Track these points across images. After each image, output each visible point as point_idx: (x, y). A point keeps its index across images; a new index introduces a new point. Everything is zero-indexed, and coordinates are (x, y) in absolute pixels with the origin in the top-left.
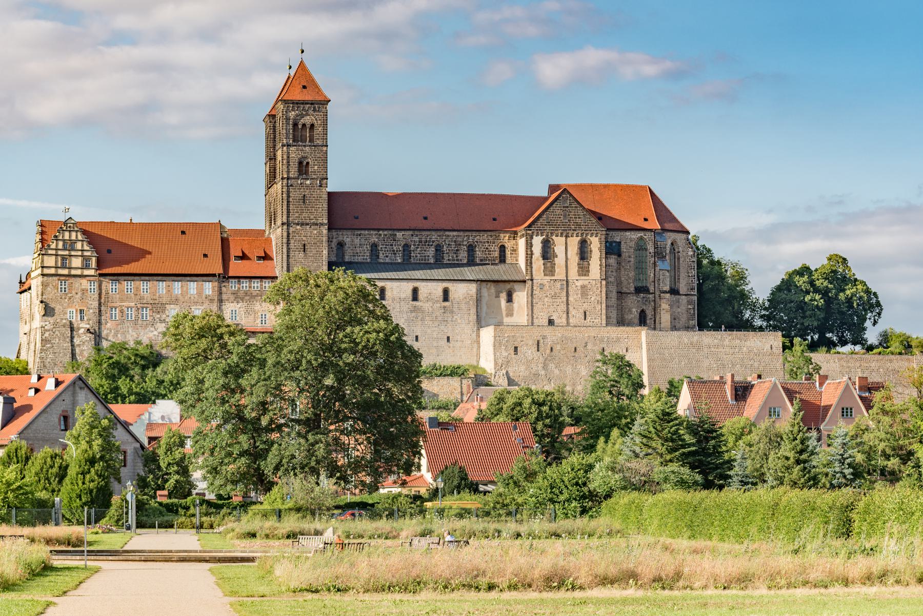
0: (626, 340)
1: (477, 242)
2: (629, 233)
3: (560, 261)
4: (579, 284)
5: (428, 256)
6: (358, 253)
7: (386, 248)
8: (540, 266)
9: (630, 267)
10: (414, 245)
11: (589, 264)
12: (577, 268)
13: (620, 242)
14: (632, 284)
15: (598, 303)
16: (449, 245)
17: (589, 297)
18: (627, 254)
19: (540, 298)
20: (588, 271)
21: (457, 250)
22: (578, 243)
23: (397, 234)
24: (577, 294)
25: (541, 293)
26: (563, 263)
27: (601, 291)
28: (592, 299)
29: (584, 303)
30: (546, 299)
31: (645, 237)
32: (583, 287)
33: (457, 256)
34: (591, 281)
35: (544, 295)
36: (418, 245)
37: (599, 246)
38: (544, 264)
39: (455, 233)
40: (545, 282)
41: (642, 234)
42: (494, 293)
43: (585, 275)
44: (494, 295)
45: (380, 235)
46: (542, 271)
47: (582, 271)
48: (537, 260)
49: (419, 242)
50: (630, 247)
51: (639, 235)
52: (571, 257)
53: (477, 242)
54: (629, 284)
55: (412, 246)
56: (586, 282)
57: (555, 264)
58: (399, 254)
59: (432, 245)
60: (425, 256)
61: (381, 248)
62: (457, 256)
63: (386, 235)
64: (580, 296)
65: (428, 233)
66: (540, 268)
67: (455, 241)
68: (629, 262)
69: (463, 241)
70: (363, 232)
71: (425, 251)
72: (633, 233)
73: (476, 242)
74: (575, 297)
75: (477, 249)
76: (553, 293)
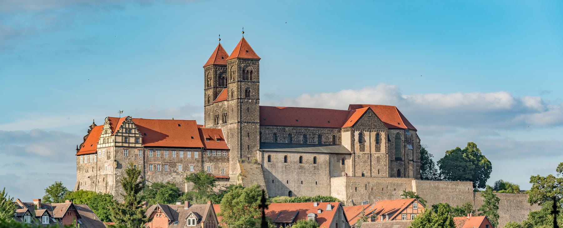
0: (405, 185)
4: (376, 156)
6: (267, 138)
7: (281, 135)
10: (294, 134)
12: (375, 148)
16: (310, 134)
17: (381, 162)
19: (358, 163)
20: (380, 149)
23: (286, 128)
24: (375, 161)
26: (369, 145)
30: (361, 163)
32: (378, 157)
33: (313, 141)
34: (382, 155)
36: (296, 134)
39: (313, 129)
41: (399, 131)
42: (336, 160)
45: (278, 129)
46: (359, 149)
51: (397, 131)
60: (299, 140)
62: (313, 141)
63: (280, 129)
65: (300, 128)
69: (316, 133)
70: (270, 127)
71: (299, 137)
72: (394, 130)
74: (374, 162)
75: (323, 137)
76: (364, 160)
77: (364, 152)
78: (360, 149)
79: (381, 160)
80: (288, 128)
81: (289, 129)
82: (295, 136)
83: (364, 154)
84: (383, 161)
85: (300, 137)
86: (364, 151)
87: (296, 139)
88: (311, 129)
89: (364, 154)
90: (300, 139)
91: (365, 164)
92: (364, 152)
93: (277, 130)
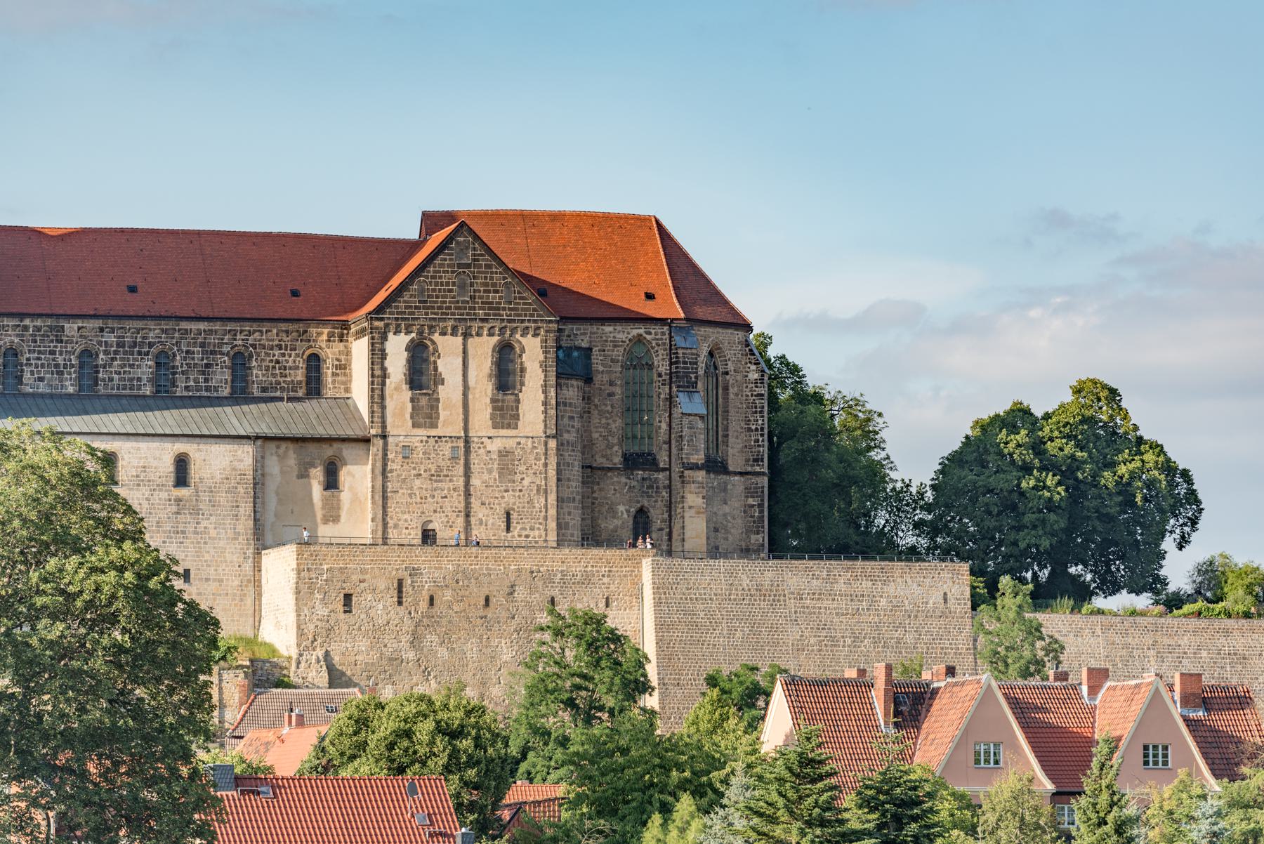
0: (606, 580)
1: (254, 346)
2: (611, 329)
3: (449, 392)
4: (494, 446)
5: (139, 379)
7: (39, 359)
8: (404, 403)
9: (612, 406)
10: (106, 353)
11: (518, 401)
12: (489, 410)
13: (590, 349)
14: (616, 448)
15: (538, 490)
16: (187, 352)
17: (518, 477)
18: (606, 378)
19: (404, 481)
20: (517, 417)
21: (207, 366)
22: (494, 351)
23: (66, 326)
24: (490, 471)
25: (406, 467)
27: (546, 465)
28: (526, 483)
29: (507, 491)
30: (417, 482)
31: (648, 337)
32: (504, 454)
33: (206, 380)
34: (523, 441)
35: (413, 472)
36: (116, 352)
37: (542, 357)
38: (412, 400)
39: (202, 326)
40: (415, 442)
41: (641, 331)
42: (296, 468)
43: (509, 426)
44: (295, 473)
45: (26, 328)
46: (408, 416)
47: (502, 416)
48: (396, 389)
49: (118, 345)
50: (612, 361)
51: (635, 332)
52: (476, 382)
53: (254, 346)
54: (610, 447)
55: (101, 356)
56: (511, 443)
57: (438, 400)
58: (70, 373)
59: (147, 354)
60: (131, 380)
61: (28, 359)
63: (38, 329)
64: (495, 474)
66: (403, 409)
67: (203, 345)
68: (611, 395)
69: (220, 345)
71: (132, 366)
72: (619, 328)
73: (252, 345)
74: (486, 476)
75: (254, 363)
76: (433, 468)
77: (433, 432)
78: (412, 417)
79: (523, 468)
80: (75, 326)
81: (79, 329)
82: (113, 359)
83: (432, 441)
84: (530, 472)
85: (139, 367)
86: (434, 426)
87: (116, 376)
88: (194, 326)
89: (432, 441)
90: (138, 373)
91: (440, 484)
92: (433, 432)
93: (18, 335)
